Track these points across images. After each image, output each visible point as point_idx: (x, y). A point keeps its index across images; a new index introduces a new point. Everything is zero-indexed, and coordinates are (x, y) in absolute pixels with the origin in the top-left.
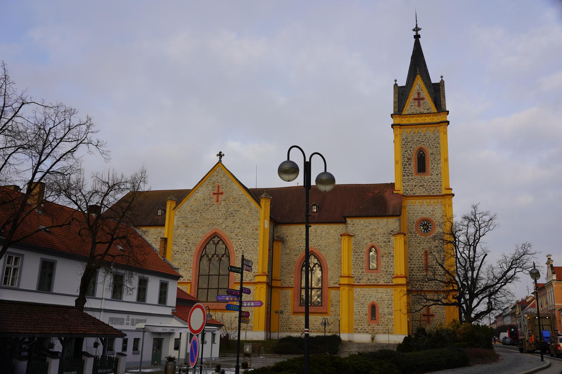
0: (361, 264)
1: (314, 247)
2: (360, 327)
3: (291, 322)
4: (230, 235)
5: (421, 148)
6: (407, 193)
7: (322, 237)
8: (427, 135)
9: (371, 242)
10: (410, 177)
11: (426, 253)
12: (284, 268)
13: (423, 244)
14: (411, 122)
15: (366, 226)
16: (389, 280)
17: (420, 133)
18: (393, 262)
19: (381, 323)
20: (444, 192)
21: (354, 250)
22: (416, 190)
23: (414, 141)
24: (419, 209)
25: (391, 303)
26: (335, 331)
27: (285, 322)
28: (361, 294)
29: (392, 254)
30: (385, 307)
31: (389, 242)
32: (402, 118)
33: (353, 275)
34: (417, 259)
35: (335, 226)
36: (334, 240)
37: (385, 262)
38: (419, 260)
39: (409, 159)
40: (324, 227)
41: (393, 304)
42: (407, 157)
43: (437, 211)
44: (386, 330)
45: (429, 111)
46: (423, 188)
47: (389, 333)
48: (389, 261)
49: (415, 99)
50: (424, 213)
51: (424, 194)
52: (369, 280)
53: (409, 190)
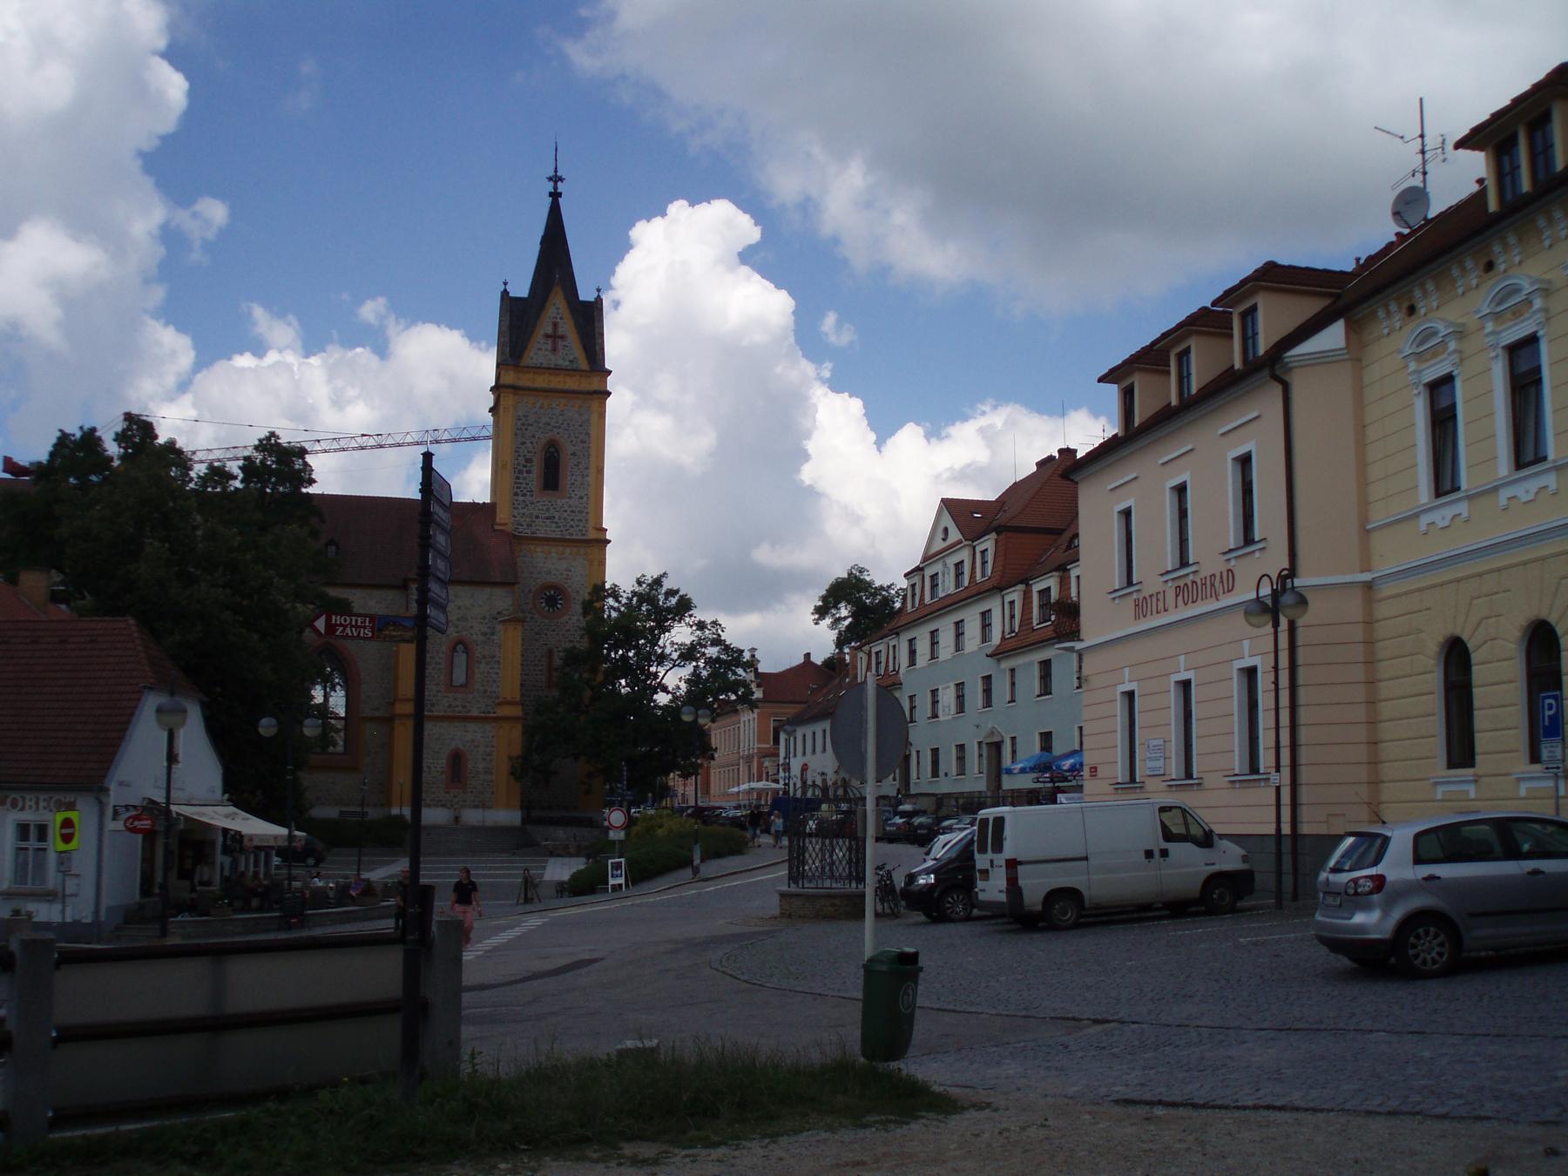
0: (436, 676)
6: (521, 530)
9: (457, 632)
10: (528, 498)
13: (546, 634)
17: (552, 408)
18: (497, 673)
20: (592, 535)
23: (540, 425)
24: (542, 565)
31: (493, 634)
38: (535, 665)
39: (528, 461)
45: (575, 366)
48: (491, 671)
49: (547, 336)
51: (553, 535)
52: (450, 706)
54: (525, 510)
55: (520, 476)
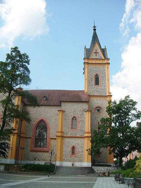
5: (97, 74)
20: (108, 94)
31: (83, 115)
39: (92, 79)
45: (101, 58)
47: (81, 161)
49: (94, 53)
51: (98, 95)
52: (72, 134)
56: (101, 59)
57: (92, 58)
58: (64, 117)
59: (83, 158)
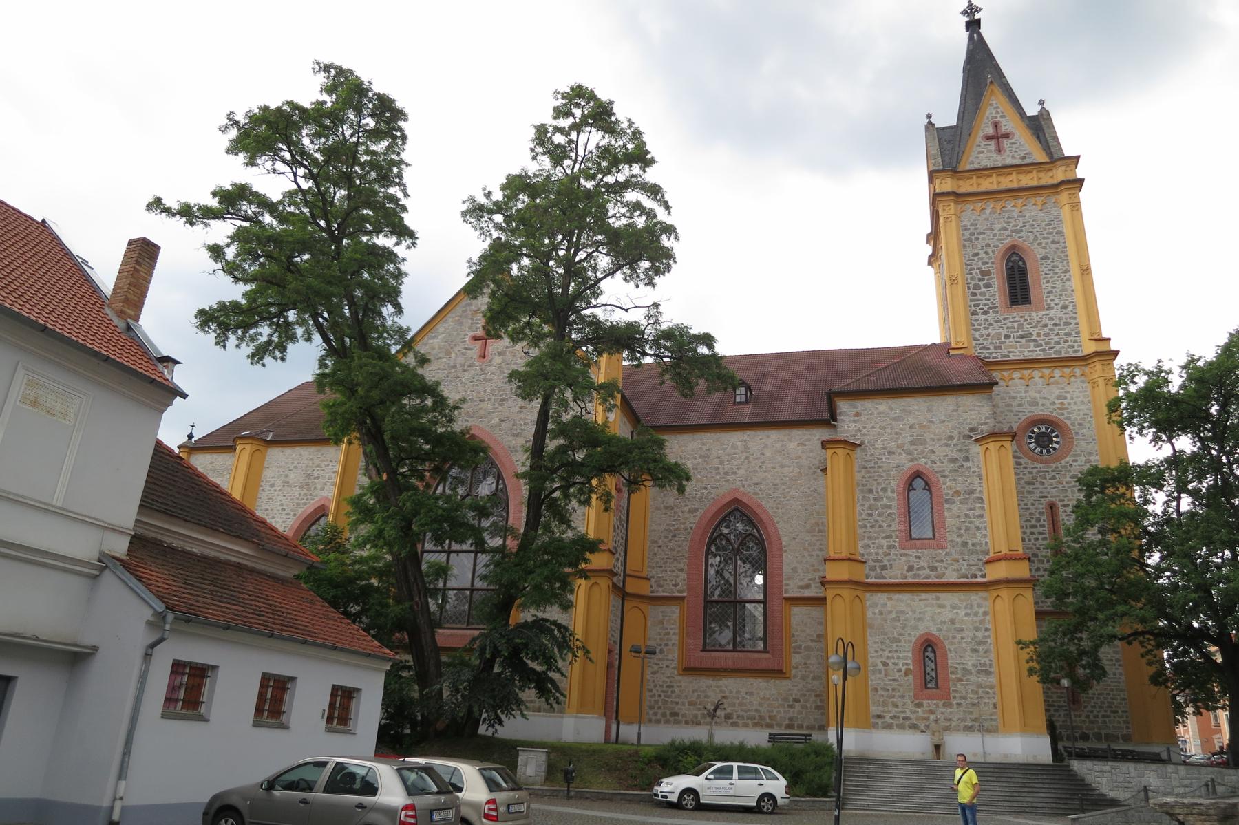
0: (885, 525)
1: (742, 489)
2: (890, 712)
3: (679, 697)
4: (510, 441)
6: (987, 355)
7: (763, 462)
8: (1028, 215)
9: (912, 461)
10: (991, 316)
11: (1051, 508)
12: (660, 547)
13: (1042, 483)
14: (982, 189)
15: (896, 419)
16: (974, 568)
18: (981, 516)
19: (954, 697)
20: (1089, 348)
21: (863, 485)
22: (1011, 346)
23: (995, 231)
24: (1023, 394)
25: (985, 637)
26: (805, 725)
27: (660, 696)
28: (890, 612)
29: (978, 495)
30: (965, 651)
31: (967, 459)
32: (959, 179)
33: (863, 555)
34: (1028, 524)
35: (800, 433)
36: (797, 470)
37: (959, 517)
38: (1033, 527)
39: (984, 273)
40: (768, 437)
41: (989, 640)
42: (978, 269)
43: (1072, 399)
44: (975, 720)
45: (1027, 161)
46: (1030, 341)
47: (984, 730)
48: (970, 513)
49: (988, 138)
50: (1037, 404)
51: (1034, 356)
52: (910, 568)
53: (991, 347)
54: (990, 330)
55: (976, 291)
56: (1027, 167)
57: (976, 166)
58: (858, 476)
59: (995, 706)
